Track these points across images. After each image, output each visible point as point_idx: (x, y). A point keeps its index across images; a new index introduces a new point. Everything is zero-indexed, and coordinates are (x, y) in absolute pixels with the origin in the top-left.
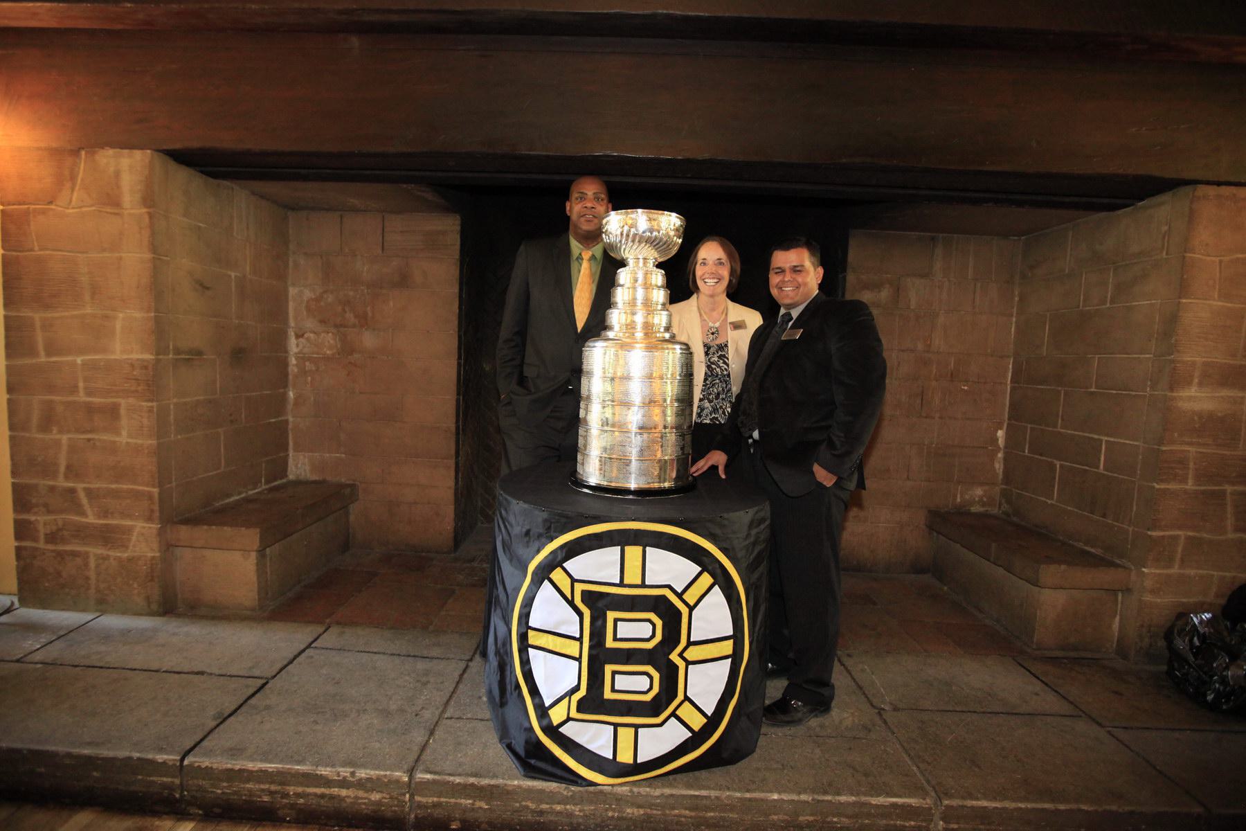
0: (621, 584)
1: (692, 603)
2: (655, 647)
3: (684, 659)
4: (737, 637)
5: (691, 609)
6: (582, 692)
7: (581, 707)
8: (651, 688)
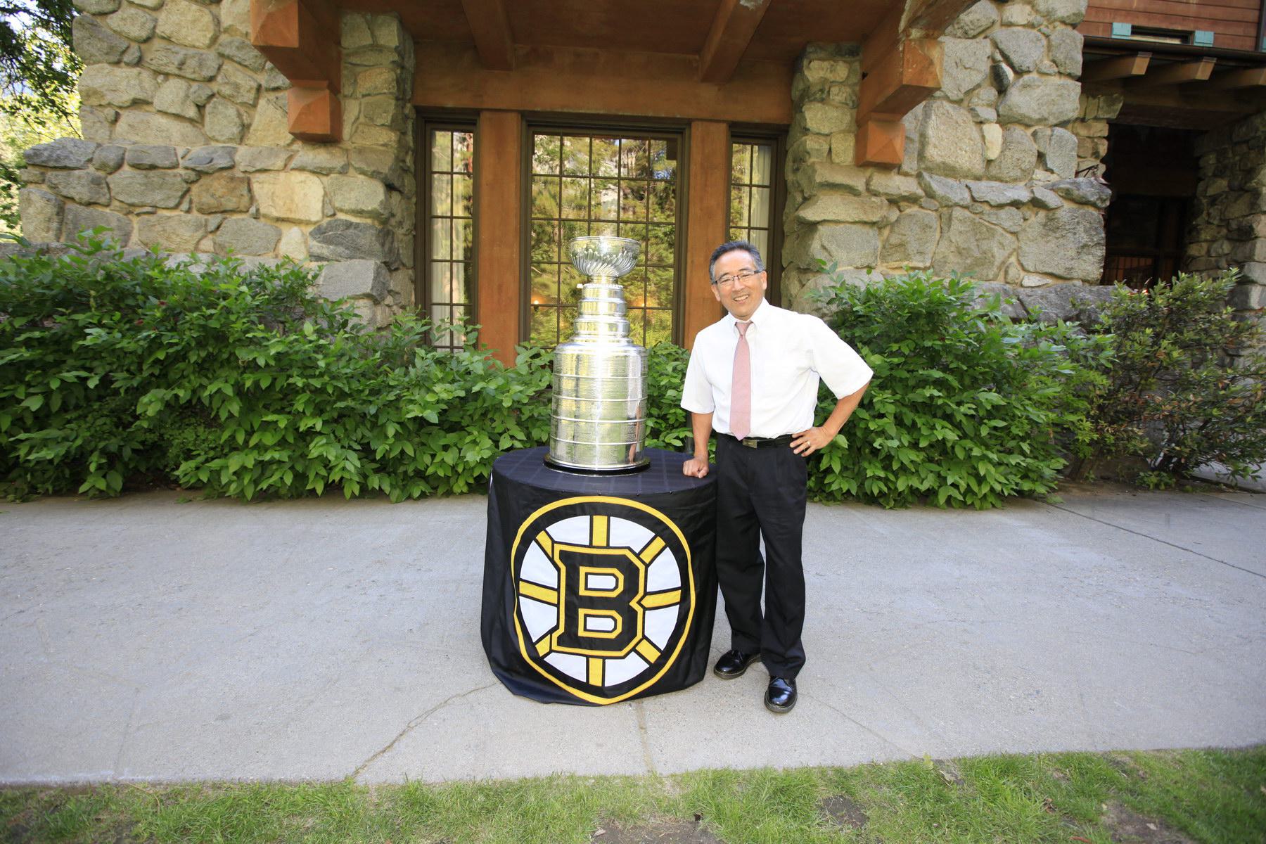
0: (591, 546)
1: (647, 562)
2: (619, 596)
3: (642, 606)
4: (684, 588)
5: (647, 566)
6: (561, 630)
7: (561, 641)
8: (615, 628)
